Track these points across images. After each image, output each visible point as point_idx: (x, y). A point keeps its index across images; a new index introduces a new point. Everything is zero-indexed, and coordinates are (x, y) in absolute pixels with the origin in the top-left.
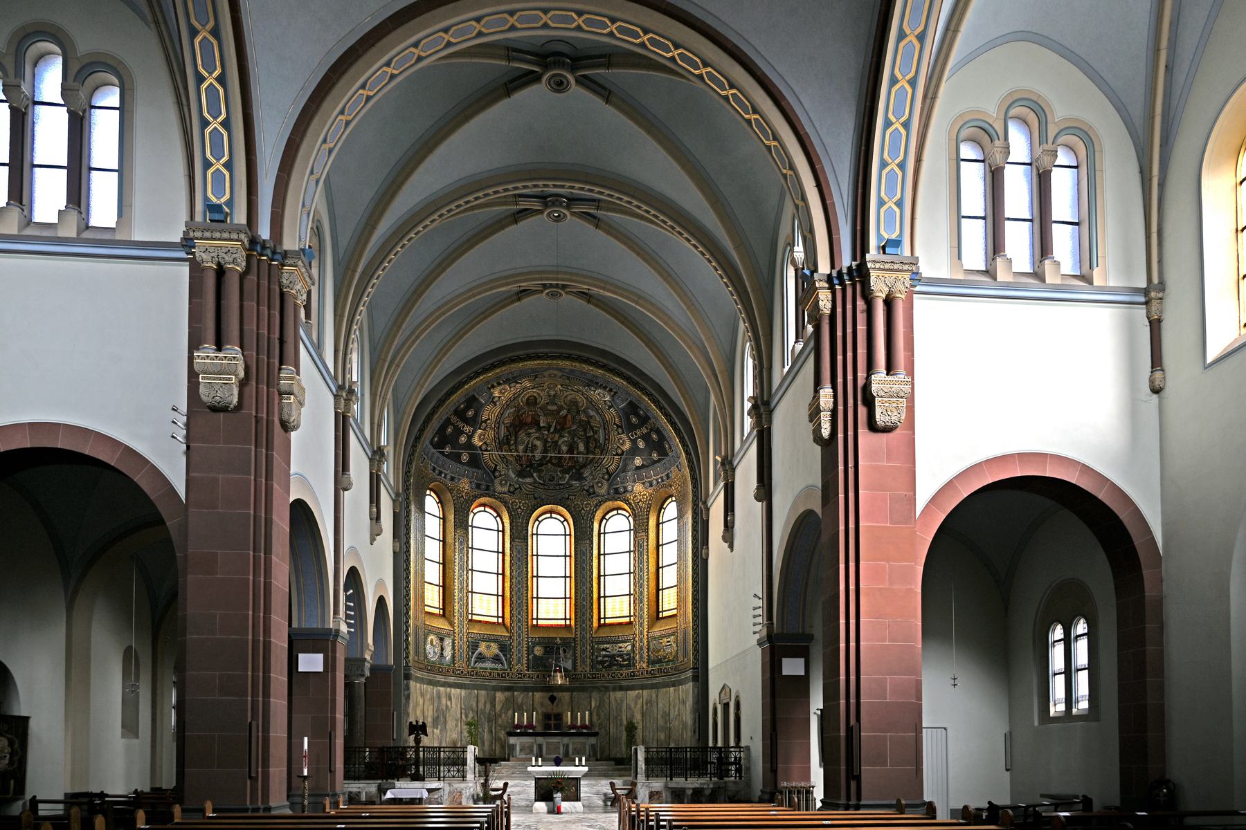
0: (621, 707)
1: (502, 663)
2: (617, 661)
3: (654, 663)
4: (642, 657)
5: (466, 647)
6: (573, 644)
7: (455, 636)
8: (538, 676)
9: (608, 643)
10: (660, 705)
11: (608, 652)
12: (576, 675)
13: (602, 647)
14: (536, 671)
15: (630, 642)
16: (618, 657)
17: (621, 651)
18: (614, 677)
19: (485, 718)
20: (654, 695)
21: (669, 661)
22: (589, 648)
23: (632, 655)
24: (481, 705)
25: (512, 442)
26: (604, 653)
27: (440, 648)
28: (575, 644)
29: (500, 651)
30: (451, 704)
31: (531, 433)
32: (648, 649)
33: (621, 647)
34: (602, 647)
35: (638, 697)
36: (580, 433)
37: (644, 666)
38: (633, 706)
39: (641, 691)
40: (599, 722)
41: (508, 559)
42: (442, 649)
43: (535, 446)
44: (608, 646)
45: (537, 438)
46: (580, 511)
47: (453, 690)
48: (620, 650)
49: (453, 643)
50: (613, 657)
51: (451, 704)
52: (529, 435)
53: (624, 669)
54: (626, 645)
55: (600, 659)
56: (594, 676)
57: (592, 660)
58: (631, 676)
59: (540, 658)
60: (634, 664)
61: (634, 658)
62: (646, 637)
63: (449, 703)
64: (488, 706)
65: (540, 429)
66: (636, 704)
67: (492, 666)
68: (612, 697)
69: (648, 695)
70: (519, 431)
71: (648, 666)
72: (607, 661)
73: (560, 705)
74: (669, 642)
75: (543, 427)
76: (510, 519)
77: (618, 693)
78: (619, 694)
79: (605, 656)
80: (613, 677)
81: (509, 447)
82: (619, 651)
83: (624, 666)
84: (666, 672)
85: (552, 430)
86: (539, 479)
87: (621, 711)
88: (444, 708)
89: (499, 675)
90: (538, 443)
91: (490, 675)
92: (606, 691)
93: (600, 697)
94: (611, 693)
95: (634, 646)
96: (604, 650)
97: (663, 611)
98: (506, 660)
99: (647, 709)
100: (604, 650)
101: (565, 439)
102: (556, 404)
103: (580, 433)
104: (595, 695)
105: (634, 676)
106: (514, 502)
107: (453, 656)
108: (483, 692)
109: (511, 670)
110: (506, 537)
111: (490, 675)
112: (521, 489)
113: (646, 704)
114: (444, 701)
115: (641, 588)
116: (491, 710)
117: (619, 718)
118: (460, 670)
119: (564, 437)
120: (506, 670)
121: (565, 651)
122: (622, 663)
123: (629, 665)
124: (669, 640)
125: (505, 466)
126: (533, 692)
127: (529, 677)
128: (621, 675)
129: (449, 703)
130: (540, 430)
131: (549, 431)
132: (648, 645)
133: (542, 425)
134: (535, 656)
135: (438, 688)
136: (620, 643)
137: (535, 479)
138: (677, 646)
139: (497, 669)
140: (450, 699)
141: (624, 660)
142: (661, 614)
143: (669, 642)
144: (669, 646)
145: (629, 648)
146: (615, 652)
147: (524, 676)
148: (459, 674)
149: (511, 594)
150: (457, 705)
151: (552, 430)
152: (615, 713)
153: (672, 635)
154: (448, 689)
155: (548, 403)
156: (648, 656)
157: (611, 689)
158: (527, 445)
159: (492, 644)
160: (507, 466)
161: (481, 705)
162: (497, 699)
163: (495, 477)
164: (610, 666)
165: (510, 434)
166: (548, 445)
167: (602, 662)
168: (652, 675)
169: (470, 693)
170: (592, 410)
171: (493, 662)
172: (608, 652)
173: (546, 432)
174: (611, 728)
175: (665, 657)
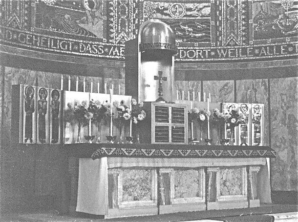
2: (184, 30)
11: (166, 14)
12: (109, 47)
14: (43, 32)
17: (190, 16)
23: (212, 23)
33: (190, 10)
39: (232, 82)
48: (189, 13)
53: (196, 44)
58: (210, 56)
61: (217, 28)
71: (247, 42)
83: (195, 39)
105: (216, 56)
123: (206, 38)
128: (191, 54)
141: (195, 31)
145: (207, 11)
156: (247, 25)
172: (166, 14)
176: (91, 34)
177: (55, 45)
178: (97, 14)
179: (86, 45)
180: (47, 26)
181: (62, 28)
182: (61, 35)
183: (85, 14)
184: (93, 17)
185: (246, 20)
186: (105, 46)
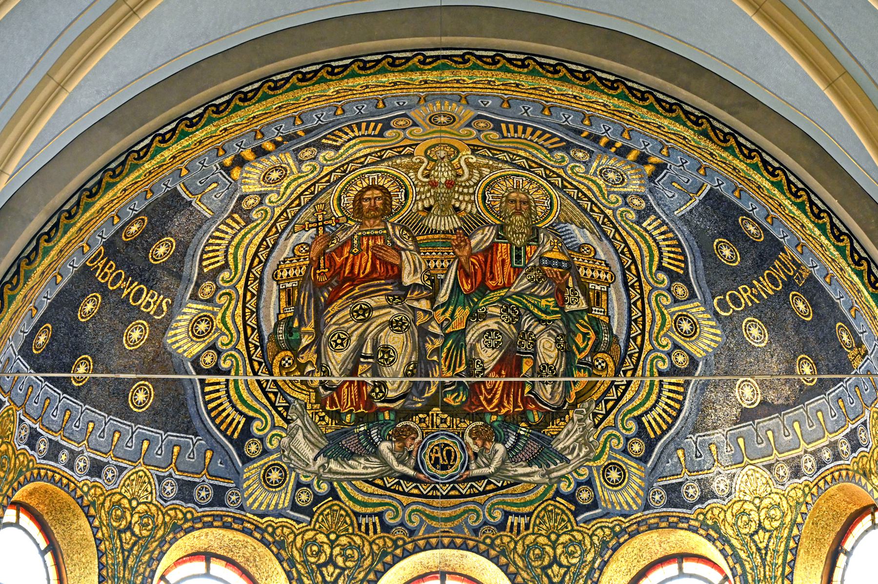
25: (305, 341)
31: (371, 309)
43: (386, 349)
45: (395, 325)
70: (329, 303)
75: (415, 286)
81: (296, 356)
85: (443, 296)
86: (401, 462)
90: (395, 340)
101: (491, 324)
102: (457, 210)
103: (543, 302)
119: (485, 316)
125: (279, 421)
131: (432, 299)
133: (408, 280)
137: (384, 462)
160: (288, 422)
163: (246, 460)
166: (429, 347)
173: (424, 305)
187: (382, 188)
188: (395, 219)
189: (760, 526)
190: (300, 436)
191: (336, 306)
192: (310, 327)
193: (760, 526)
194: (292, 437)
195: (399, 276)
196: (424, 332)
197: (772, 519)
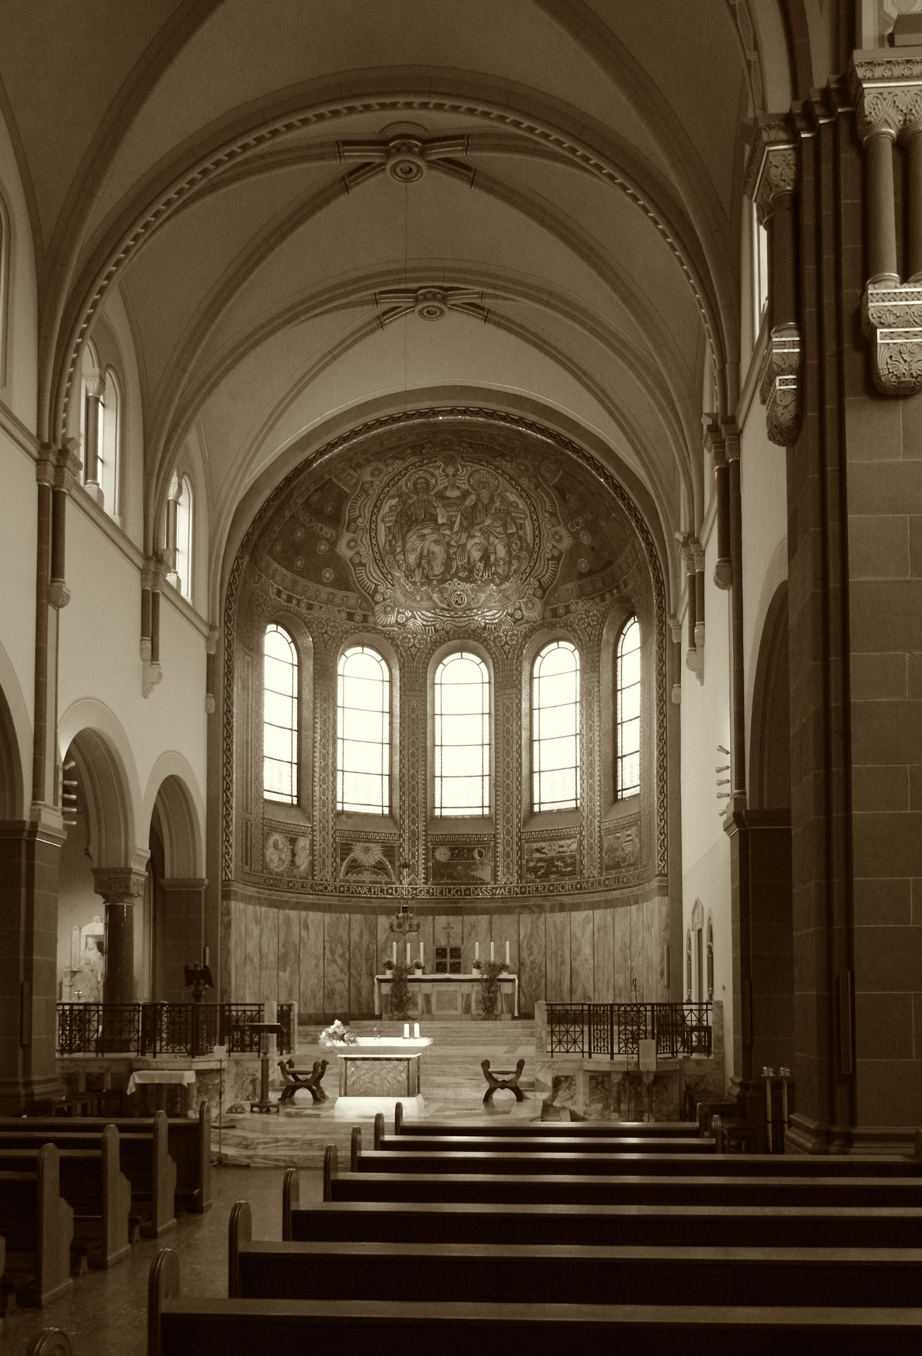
0: (562, 936)
1: (387, 874)
2: (557, 867)
3: (609, 868)
4: (591, 860)
5: (331, 850)
6: (492, 843)
7: (313, 836)
8: (441, 893)
9: (544, 841)
10: (618, 933)
12: (496, 889)
13: (535, 846)
14: (438, 884)
15: (575, 837)
16: (557, 861)
17: (562, 852)
18: (553, 891)
19: (361, 955)
20: (609, 918)
21: (629, 865)
22: (515, 848)
23: (578, 857)
24: (355, 936)
25: (398, 550)
26: (538, 855)
27: (289, 853)
28: (496, 843)
29: (385, 856)
30: (308, 934)
31: (425, 535)
32: (601, 847)
33: (562, 846)
34: (535, 846)
35: (586, 921)
36: (498, 530)
37: (595, 873)
38: (579, 934)
39: (591, 912)
40: (531, 958)
41: (397, 721)
42: (294, 855)
43: (433, 553)
44: (543, 844)
45: (436, 542)
46: (502, 647)
47: (311, 914)
48: (561, 850)
49: (312, 844)
50: (550, 861)
51: (308, 934)
52: (423, 537)
53: (567, 878)
54: (568, 842)
55: (532, 864)
56: (523, 890)
57: (520, 867)
58: (577, 889)
59: (446, 865)
60: (581, 871)
62: (597, 829)
63: (304, 933)
64: (366, 937)
65: (438, 527)
66: (583, 933)
67: (373, 878)
68: (550, 922)
69: (601, 918)
70: (407, 532)
71: (600, 874)
72: (542, 867)
73: (473, 934)
74: (629, 835)
75: (443, 524)
76: (400, 662)
77: (558, 914)
78: (559, 917)
79: (541, 860)
80: (551, 892)
81: (395, 557)
82: (559, 852)
84: (626, 883)
85: (456, 527)
86: (442, 602)
87: (563, 942)
88: (297, 941)
89: (382, 891)
90: (436, 549)
91: (370, 891)
92: (541, 913)
93: (532, 922)
94: (548, 915)
95: (580, 843)
96: (538, 850)
97: (623, 790)
98: (393, 869)
99: (599, 938)
100: (538, 850)
101: (477, 540)
102: (458, 488)
103: (498, 530)
104: (526, 919)
105: (581, 888)
106: (406, 637)
107: (312, 864)
108: (358, 917)
109: (401, 884)
110: (394, 690)
111: (370, 891)
112: (415, 618)
113: (599, 931)
114: (295, 930)
115: (591, 755)
116: (370, 942)
117: (560, 952)
118: (322, 885)
119: (473, 537)
120: (394, 883)
121: (480, 854)
122: (564, 870)
123: (572, 873)
124: (629, 832)
125: (389, 586)
126: (434, 915)
127: (428, 892)
128: (563, 887)
129: (304, 933)
130: (438, 530)
131: (451, 529)
132: (601, 841)
133: (440, 521)
134: (437, 862)
135: (287, 911)
136: (560, 840)
137: (435, 603)
138: (640, 841)
139: (380, 883)
140: (306, 927)
141: (567, 866)
142: (620, 793)
143: (629, 835)
144: (629, 843)
145: (574, 846)
146: (553, 854)
147: (420, 891)
148: (321, 891)
149: (400, 772)
150: (317, 936)
151: (456, 527)
152: (554, 945)
153: (633, 826)
154: (303, 913)
155: (446, 488)
156: (601, 858)
157: (547, 909)
158: (421, 554)
159: (373, 845)
160: (393, 585)
161: (355, 936)
162: (379, 927)
163: (377, 603)
164: (546, 875)
165: (394, 537)
166: (451, 552)
167: (535, 870)
168: (606, 886)
169: (338, 919)
170: (512, 493)
171: (375, 873)
173: (448, 532)
174: (548, 967)
175: (624, 860)
176: (480, 879)
177: (450, 892)
178: (486, 861)
179: (476, 889)
180: (442, 878)
181: (455, 878)
182: (454, 884)
183: (474, 864)
184: (482, 864)
185: (600, 852)
186: (493, 888)
187: (425, 478)
188: (432, 493)
189: (589, 624)
190: (398, 592)
191: (410, 534)
192: (400, 543)
193: (589, 624)
194: (394, 591)
195: (436, 520)
196: (449, 545)
197: (593, 621)
